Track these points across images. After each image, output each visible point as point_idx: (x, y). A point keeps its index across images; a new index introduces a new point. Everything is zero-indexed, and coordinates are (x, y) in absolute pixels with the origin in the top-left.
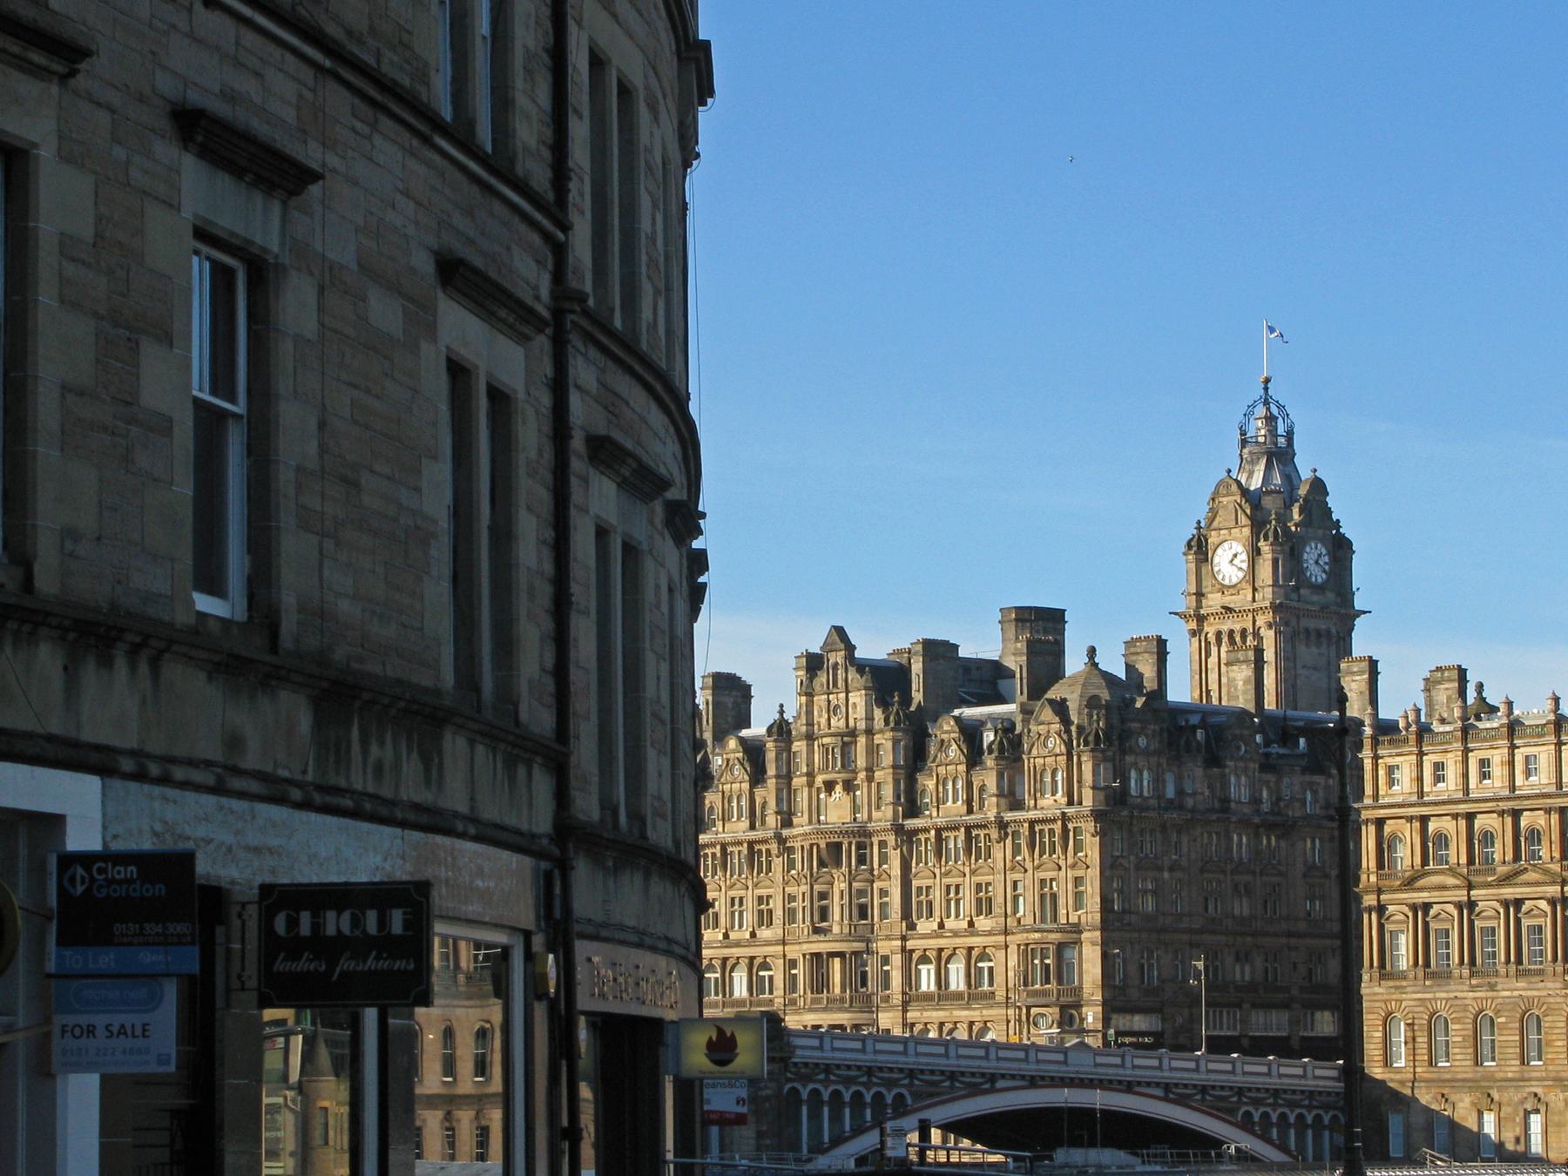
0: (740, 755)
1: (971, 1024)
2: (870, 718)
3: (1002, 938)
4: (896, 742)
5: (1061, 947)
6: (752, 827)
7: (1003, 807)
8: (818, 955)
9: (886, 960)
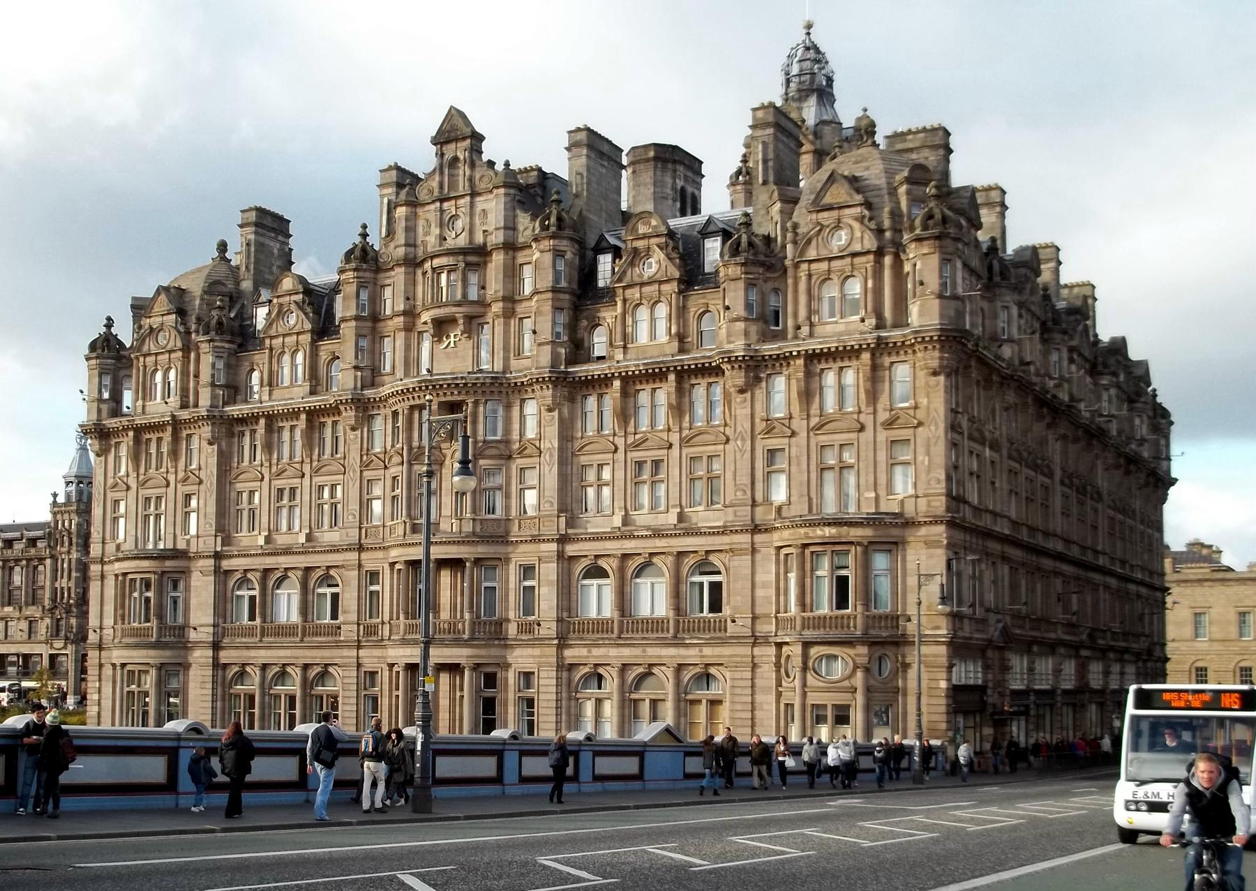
0: (299, 297)
1: (680, 668)
2: (510, 226)
3: (746, 538)
4: (558, 254)
5: (869, 548)
6: (313, 392)
7: (754, 337)
8: (414, 564)
9: (528, 571)
